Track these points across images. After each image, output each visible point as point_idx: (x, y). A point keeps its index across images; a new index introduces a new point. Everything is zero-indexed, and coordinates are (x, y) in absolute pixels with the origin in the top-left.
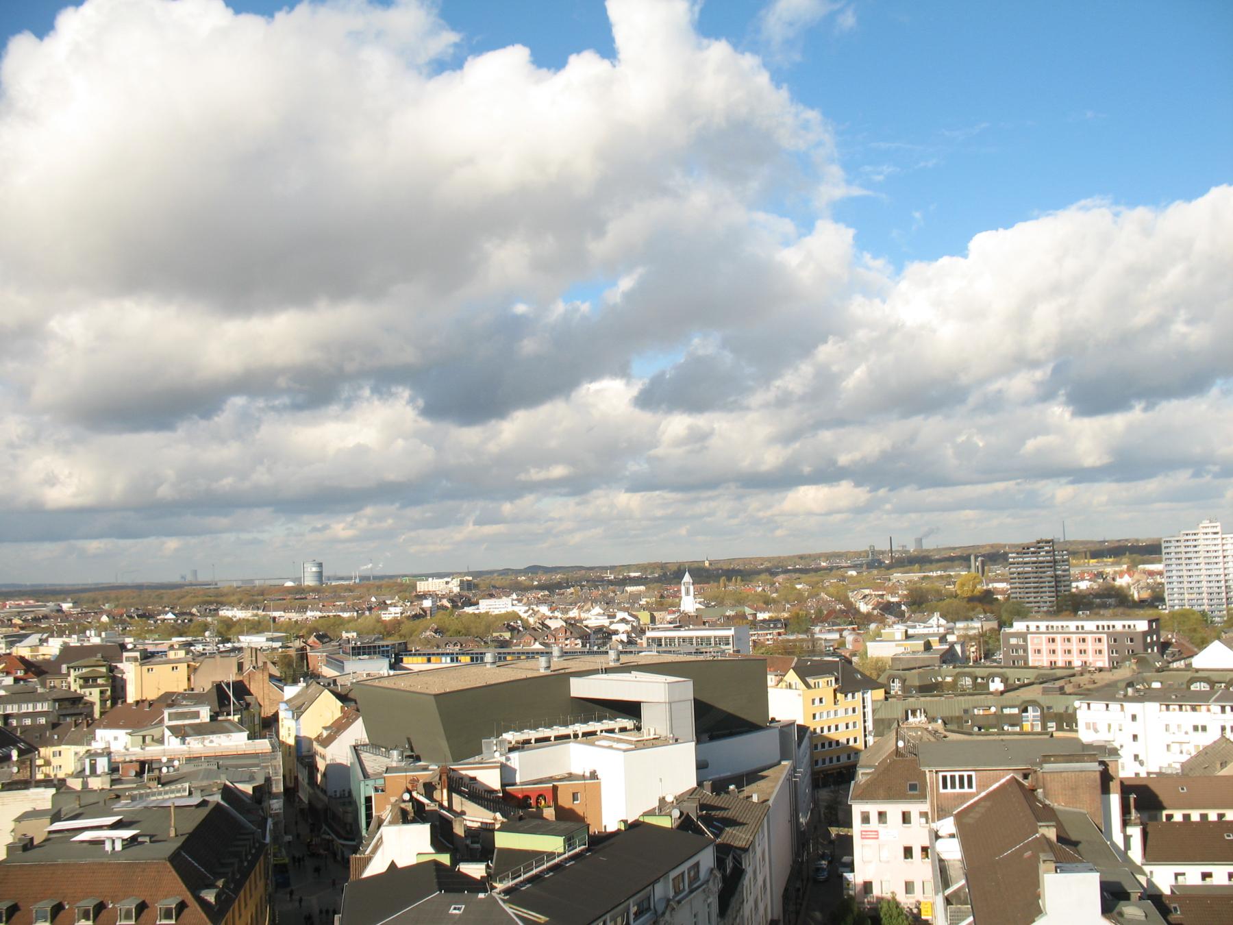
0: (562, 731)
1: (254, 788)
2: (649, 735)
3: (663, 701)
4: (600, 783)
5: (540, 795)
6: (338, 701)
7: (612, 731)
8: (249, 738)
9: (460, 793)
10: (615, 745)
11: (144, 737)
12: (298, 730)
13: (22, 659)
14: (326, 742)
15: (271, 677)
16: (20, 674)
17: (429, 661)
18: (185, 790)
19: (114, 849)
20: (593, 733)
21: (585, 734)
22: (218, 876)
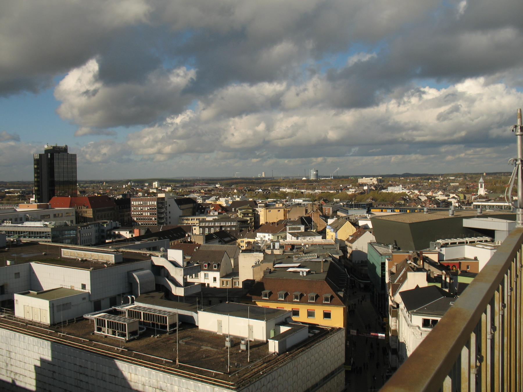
0: (461, 240)
1: (339, 257)
2: (499, 244)
3: (505, 229)
4: (479, 262)
5: (454, 266)
6: (352, 226)
7: (481, 241)
8: (322, 239)
9: (426, 262)
10: (485, 247)
11: (278, 237)
12: (336, 236)
13: (220, 205)
14: (352, 241)
15: (320, 215)
16: (220, 211)
17: (382, 211)
18: (315, 256)
19: (303, 275)
20: (474, 242)
21: (471, 242)
22: (342, 287)
